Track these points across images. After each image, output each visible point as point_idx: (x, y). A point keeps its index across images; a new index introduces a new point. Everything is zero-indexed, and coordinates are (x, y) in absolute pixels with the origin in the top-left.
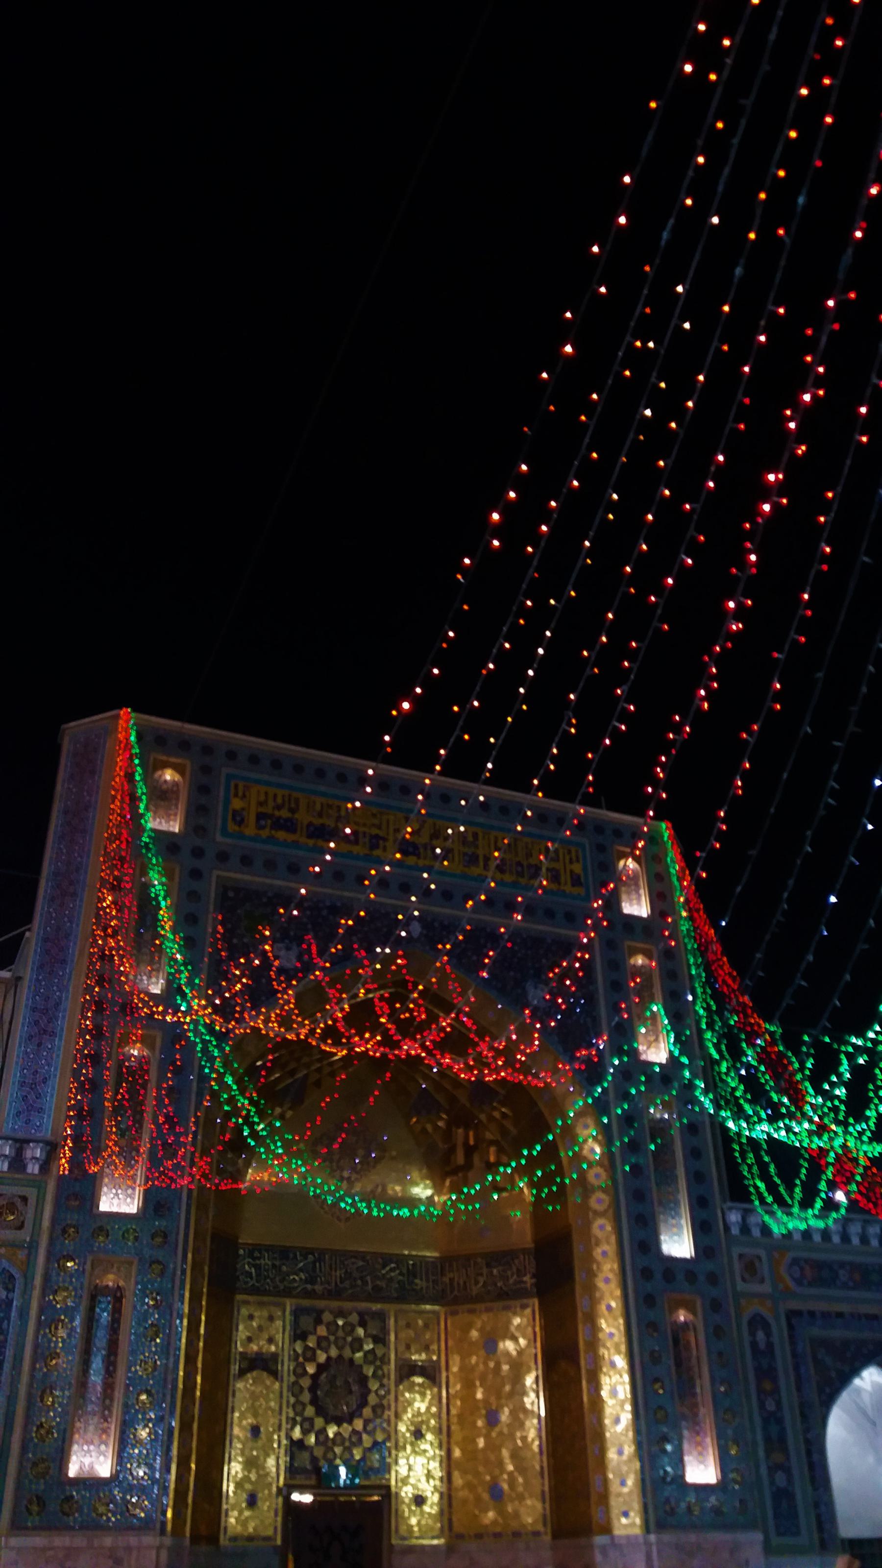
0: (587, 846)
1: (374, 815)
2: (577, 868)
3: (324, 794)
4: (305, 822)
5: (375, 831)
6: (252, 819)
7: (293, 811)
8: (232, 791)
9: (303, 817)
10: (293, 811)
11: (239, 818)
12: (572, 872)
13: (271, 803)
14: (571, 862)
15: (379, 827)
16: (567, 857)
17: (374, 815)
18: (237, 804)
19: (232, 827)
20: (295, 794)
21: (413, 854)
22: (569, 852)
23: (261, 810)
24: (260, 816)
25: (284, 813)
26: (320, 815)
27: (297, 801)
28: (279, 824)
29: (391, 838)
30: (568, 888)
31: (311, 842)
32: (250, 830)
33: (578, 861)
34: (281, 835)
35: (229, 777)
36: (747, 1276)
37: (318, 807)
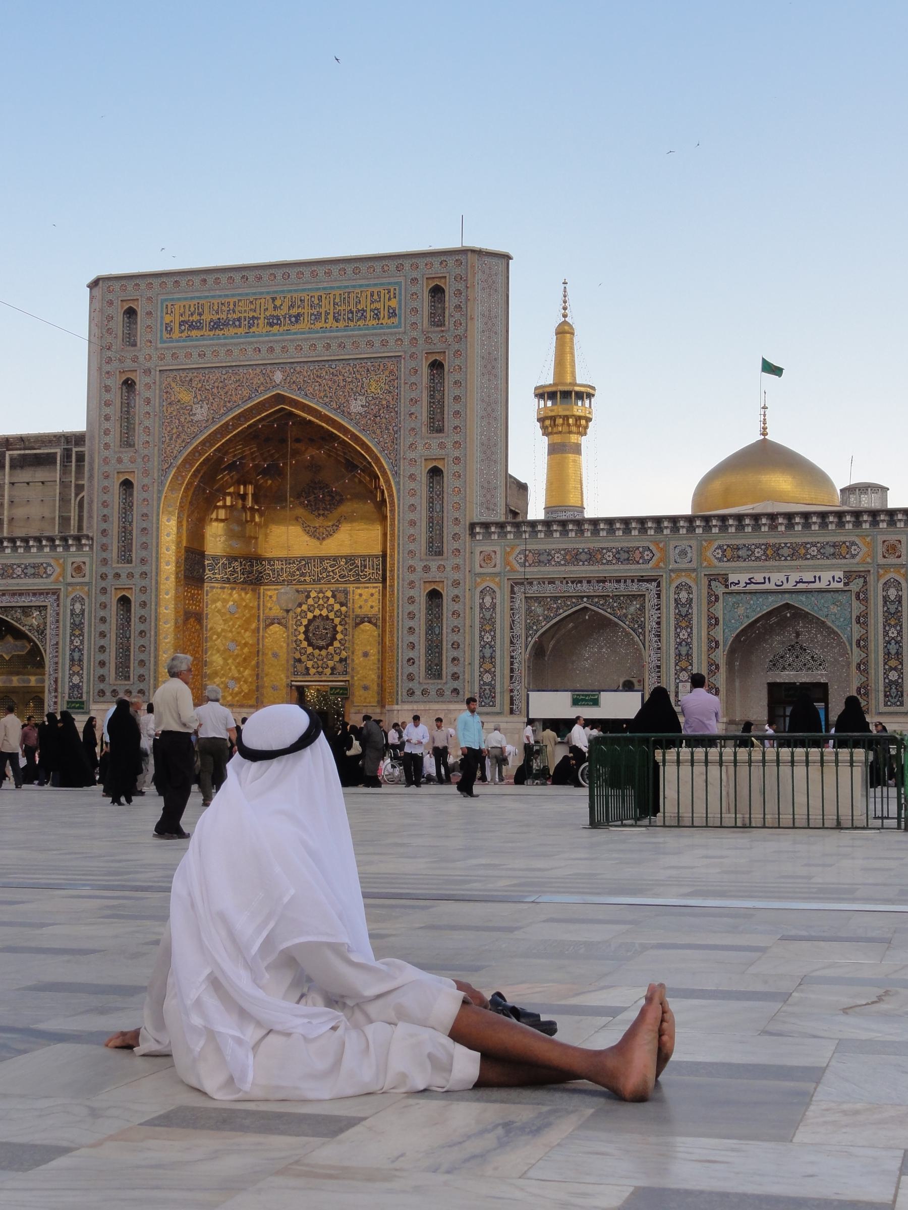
0: (403, 284)
1: (251, 302)
2: (394, 303)
3: (220, 296)
4: (208, 320)
5: (251, 314)
6: (177, 325)
7: (200, 314)
8: (165, 310)
9: (207, 317)
10: (200, 314)
11: (169, 328)
12: (389, 306)
13: (188, 313)
14: (389, 299)
15: (255, 311)
16: (387, 296)
17: (251, 302)
18: (168, 319)
19: (166, 335)
20: (201, 302)
21: (277, 324)
22: (389, 292)
23: (182, 319)
24: (182, 323)
25: (196, 317)
26: (217, 313)
27: (203, 305)
28: (192, 327)
29: (262, 316)
31: (212, 333)
32: (176, 335)
33: (395, 297)
34: (194, 333)
35: (163, 301)
36: (483, 564)
37: (216, 308)
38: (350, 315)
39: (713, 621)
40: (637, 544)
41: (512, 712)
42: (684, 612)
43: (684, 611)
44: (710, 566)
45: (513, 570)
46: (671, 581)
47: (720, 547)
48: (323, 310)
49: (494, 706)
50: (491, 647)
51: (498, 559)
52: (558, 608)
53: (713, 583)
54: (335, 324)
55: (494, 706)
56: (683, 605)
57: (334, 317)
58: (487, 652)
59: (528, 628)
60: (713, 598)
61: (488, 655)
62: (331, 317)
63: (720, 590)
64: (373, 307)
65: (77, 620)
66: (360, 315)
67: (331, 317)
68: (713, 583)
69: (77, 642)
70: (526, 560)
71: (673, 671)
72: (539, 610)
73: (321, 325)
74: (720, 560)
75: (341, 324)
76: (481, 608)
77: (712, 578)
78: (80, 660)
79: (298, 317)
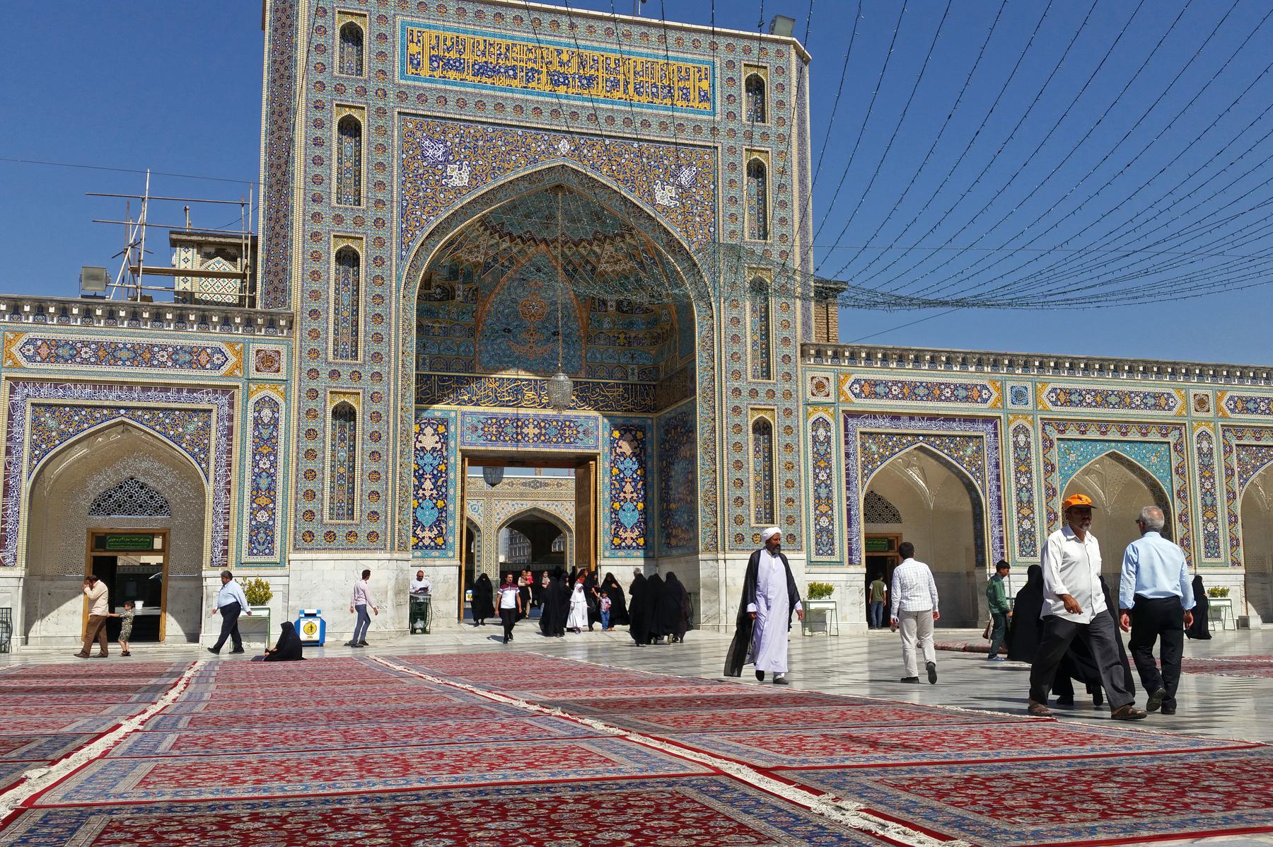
30: (696, 104)
38: (654, 90)
39: (1050, 468)
40: (975, 382)
41: (851, 562)
42: (266, 435)
43: (822, 450)
44: (1045, 410)
45: (847, 401)
46: (1009, 423)
47: (1054, 390)
48: (621, 77)
49: (833, 554)
50: (827, 486)
51: (831, 387)
52: (894, 447)
53: (1047, 427)
54: (636, 98)
55: (833, 554)
56: (822, 443)
57: (636, 89)
58: (264, 483)
59: (864, 467)
60: (1048, 444)
61: (823, 495)
62: (631, 87)
63: (1055, 435)
64: (681, 84)
65: (822, 450)
66: (666, 91)
67: (631, 87)
68: (1047, 427)
69: (1024, 481)
70: (1058, 399)
71: (1015, 521)
72: (874, 448)
73: (620, 94)
74: (1055, 404)
75: (645, 99)
76: (256, 424)
77: (1046, 422)
78: (829, 498)
79: (591, 79)
